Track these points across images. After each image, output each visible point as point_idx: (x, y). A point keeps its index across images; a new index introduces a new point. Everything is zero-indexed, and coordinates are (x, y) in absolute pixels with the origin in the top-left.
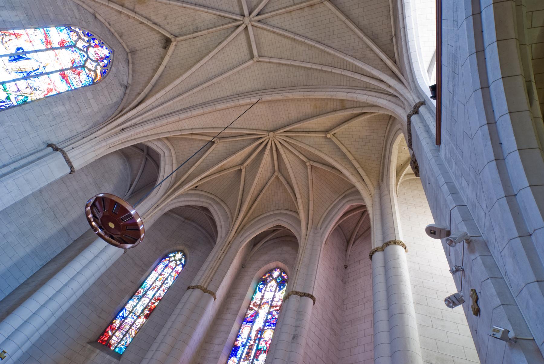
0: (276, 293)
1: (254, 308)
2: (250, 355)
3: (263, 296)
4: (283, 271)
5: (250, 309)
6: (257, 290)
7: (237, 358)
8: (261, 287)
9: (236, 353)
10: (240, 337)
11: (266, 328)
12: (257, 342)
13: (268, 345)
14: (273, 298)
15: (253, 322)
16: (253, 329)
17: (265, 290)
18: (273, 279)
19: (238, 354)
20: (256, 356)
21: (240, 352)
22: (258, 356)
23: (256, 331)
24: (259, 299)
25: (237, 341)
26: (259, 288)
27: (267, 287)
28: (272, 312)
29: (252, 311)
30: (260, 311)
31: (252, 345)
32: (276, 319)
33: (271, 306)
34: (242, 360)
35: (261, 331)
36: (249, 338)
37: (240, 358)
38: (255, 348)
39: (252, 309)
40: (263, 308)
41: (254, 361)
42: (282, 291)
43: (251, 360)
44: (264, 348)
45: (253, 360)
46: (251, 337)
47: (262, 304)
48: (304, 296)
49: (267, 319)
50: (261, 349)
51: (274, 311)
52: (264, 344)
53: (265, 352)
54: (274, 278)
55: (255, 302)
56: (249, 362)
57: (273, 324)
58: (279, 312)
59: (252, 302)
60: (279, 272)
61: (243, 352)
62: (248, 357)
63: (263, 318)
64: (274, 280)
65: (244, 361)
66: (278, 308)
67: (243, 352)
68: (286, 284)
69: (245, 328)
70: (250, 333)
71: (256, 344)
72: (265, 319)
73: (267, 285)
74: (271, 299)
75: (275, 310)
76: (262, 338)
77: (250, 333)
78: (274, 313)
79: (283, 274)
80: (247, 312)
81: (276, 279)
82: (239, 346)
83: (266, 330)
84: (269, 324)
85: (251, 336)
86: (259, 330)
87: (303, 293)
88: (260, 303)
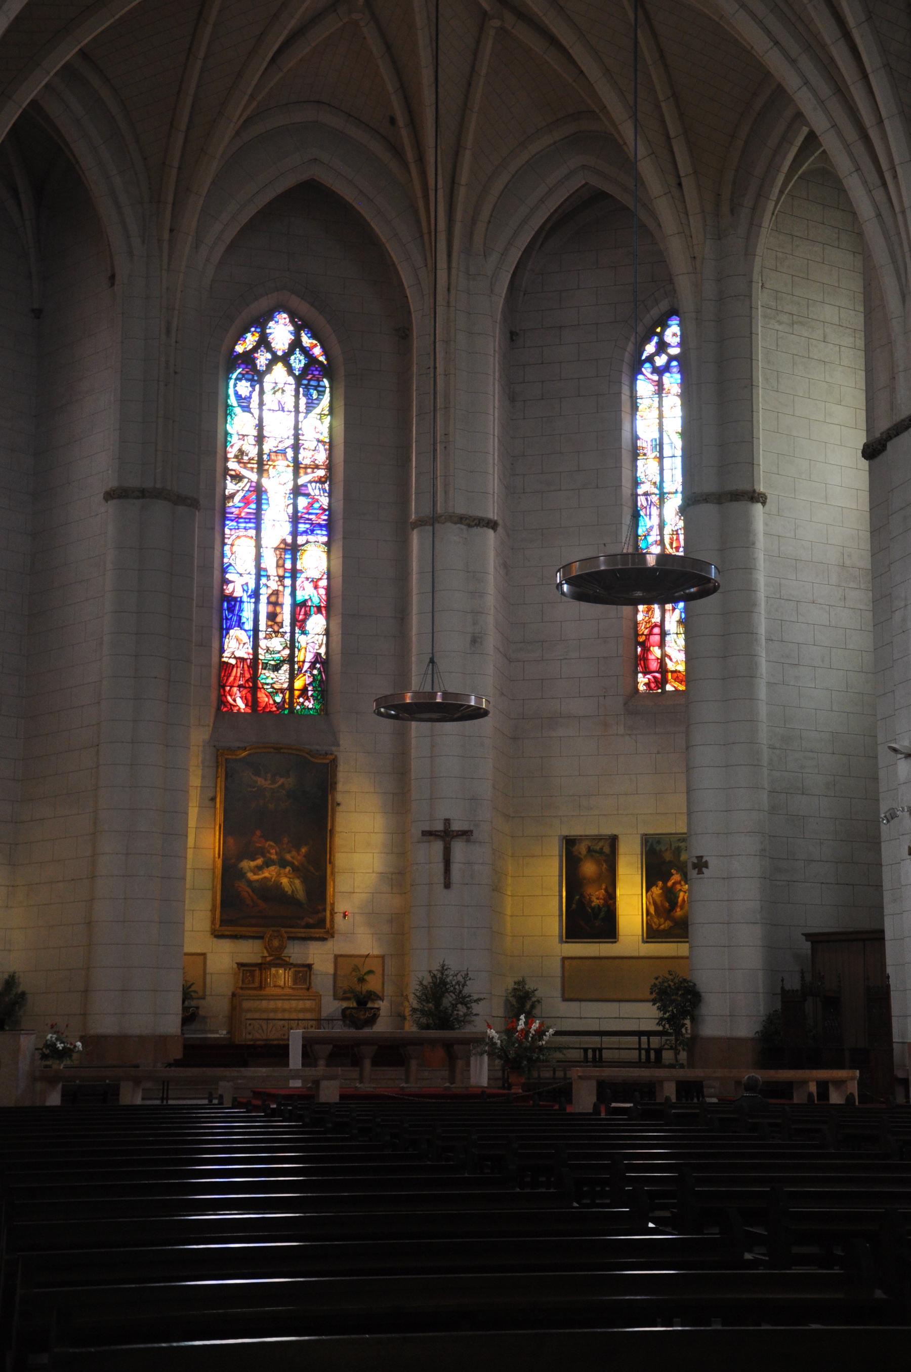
0: (301, 416)
1: (244, 472)
2: (279, 619)
3: (260, 427)
4: (300, 324)
5: (233, 477)
6: (232, 401)
7: (246, 631)
8: (244, 388)
9: (240, 617)
10: (231, 569)
11: (301, 540)
12: (288, 582)
13: (322, 592)
14: (297, 437)
15: (257, 519)
16: (264, 542)
17: (261, 404)
18: (274, 354)
19: (243, 620)
20: (299, 623)
21: (247, 613)
22: (304, 621)
23: (276, 549)
24: (252, 440)
25: (229, 582)
26: (236, 393)
27: (262, 392)
28: (305, 486)
29: (241, 484)
30: (265, 482)
31: (276, 593)
32: (325, 510)
33: (297, 466)
34: (262, 635)
35: (292, 549)
36: (260, 572)
37: (256, 630)
38: (287, 601)
39: (238, 478)
40: (272, 471)
41: (297, 635)
42: (318, 410)
43: (288, 635)
44: (313, 599)
45: (293, 633)
46: (265, 570)
47: (265, 457)
48: (477, 525)
49: (295, 510)
50: (304, 604)
51: (310, 482)
52: (309, 587)
53: (319, 610)
54: (280, 353)
55: (241, 452)
56: (282, 640)
57: (320, 526)
58: (326, 486)
59: (229, 449)
60: (291, 328)
61: (256, 613)
62: (276, 628)
63: (283, 506)
64: (280, 365)
65: (268, 637)
66: (321, 473)
67: (256, 613)
68: (326, 382)
69: (237, 542)
70: (258, 557)
71: (288, 591)
72: (290, 510)
73: (261, 382)
74: (291, 441)
75: (316, 482)
76: (301, 572)
77: (258, 557)
78: (313, 489)
79: (306, 340)
80: (225, 488)
81: (285, 359)
82: (241, 597)
83: (303, 545)
84: (308, 526)
85: (263, 566)
86: (282, 546)
87: (474, 520)
88: (260, 453)
